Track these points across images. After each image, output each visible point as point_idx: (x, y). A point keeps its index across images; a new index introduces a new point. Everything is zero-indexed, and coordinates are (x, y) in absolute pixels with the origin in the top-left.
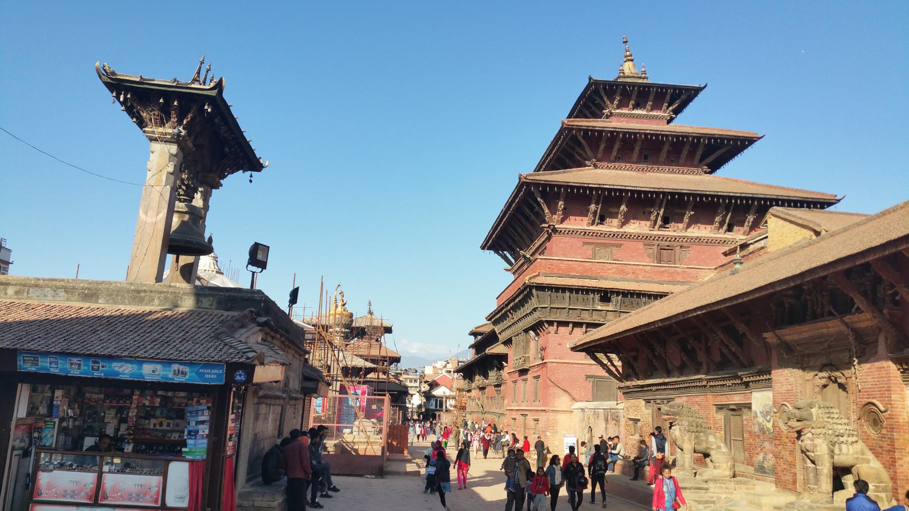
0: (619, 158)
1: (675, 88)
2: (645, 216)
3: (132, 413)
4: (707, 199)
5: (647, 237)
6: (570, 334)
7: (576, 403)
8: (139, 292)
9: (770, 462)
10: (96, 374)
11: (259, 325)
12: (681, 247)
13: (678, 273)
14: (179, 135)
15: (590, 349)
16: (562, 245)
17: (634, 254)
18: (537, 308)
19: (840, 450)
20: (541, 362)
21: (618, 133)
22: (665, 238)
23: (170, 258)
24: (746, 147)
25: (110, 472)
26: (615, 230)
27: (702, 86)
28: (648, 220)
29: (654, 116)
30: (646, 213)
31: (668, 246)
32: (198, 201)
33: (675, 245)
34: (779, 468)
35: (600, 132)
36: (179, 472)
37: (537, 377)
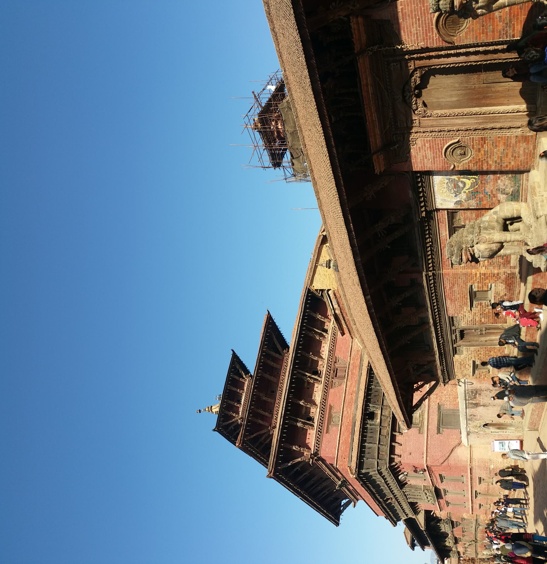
2: (311, 387)
5: (326, 386)
6: (401, 445)
7: (463, 442)
9: (506, 183)
12: (335, 362)
13: (354, 363)
16: (327, 450)
18: (378, 471)
20: (427, 472)
22: (328, 373)
26: (318, 409)
27: (232, 352)
28: (313, 385)
30: (308, 387)
31: (334, 372)
33: (334, 367)
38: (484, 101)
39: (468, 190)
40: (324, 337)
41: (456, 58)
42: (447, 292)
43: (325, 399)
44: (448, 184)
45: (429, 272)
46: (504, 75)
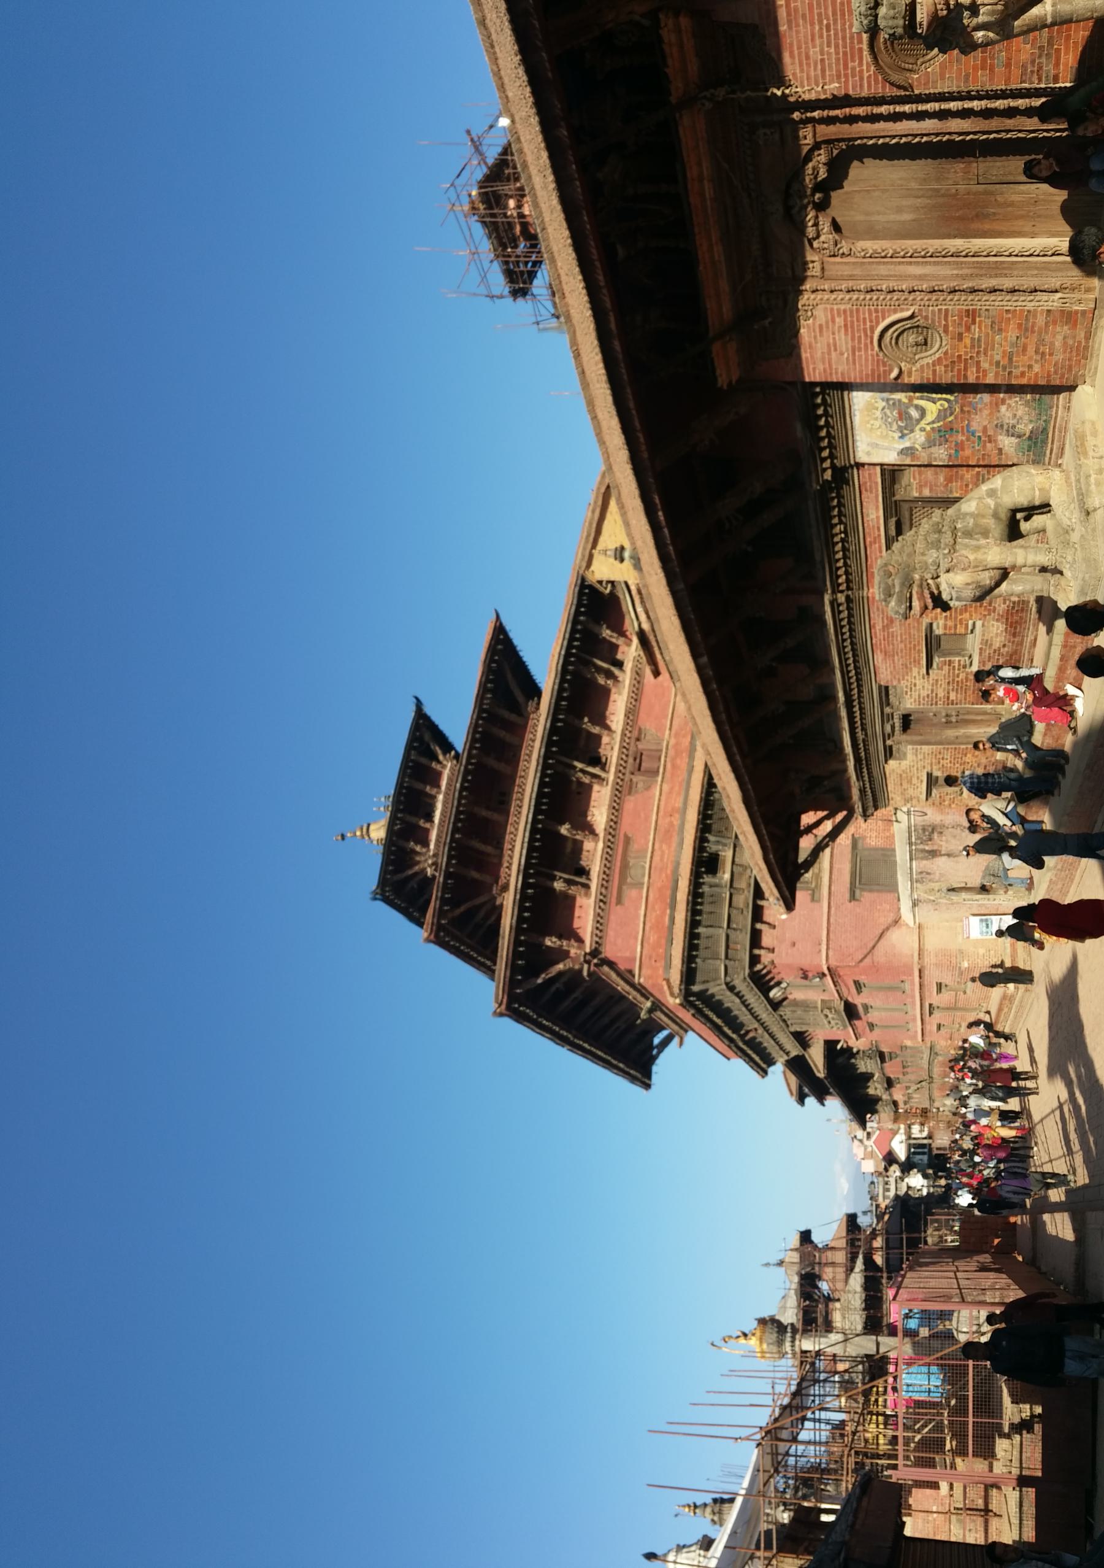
2: (584, 793)
6: (774, 927)
7: (903, 917)
9: (1020, 413)
12: (638, 740)
13: (677, 744)
17: (642, 815)
20: (829, 978)
22: (622, 762)
26: (601, 845)
34: (1037, 368)
38: (975, 225)
39: (931, 426)
40: (615, 678)
41: (914, 122)
42: (876, 637)
43: (614, 823)
44: (886, 410)
45: (839, 595)
46: (1028, 172)
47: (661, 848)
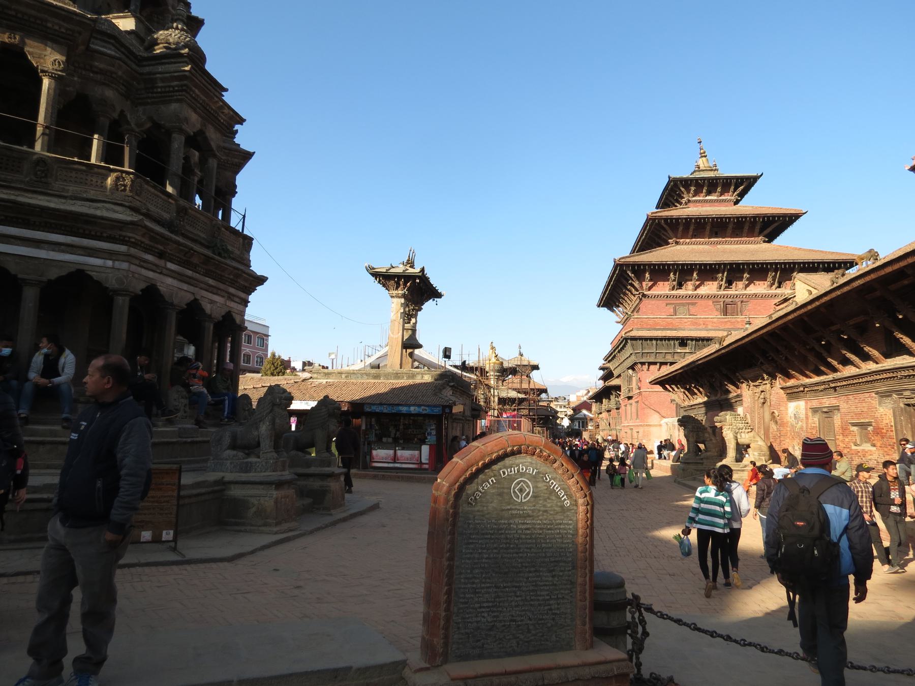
0: (695, 235)
1: (737, 178)
3: (401, 427)
4: (758, 266)
8: (397, 374)
10: (393, 411)
11: (451, 386)
13: (738, 322)
14: (405, 294)
15: (663, 382)
16: (650, 306)
19: (741, 436)
21: (691, 219)
23: (404, 350)
24: (795, 221)
25: (399, 450)
26: (690, 292)
27: (759, 175)
29: (723, 200)
32: (407, 309)
35: (677, 219)
36: (425, 449)
37: (637, 402)
47: (689, 321)
